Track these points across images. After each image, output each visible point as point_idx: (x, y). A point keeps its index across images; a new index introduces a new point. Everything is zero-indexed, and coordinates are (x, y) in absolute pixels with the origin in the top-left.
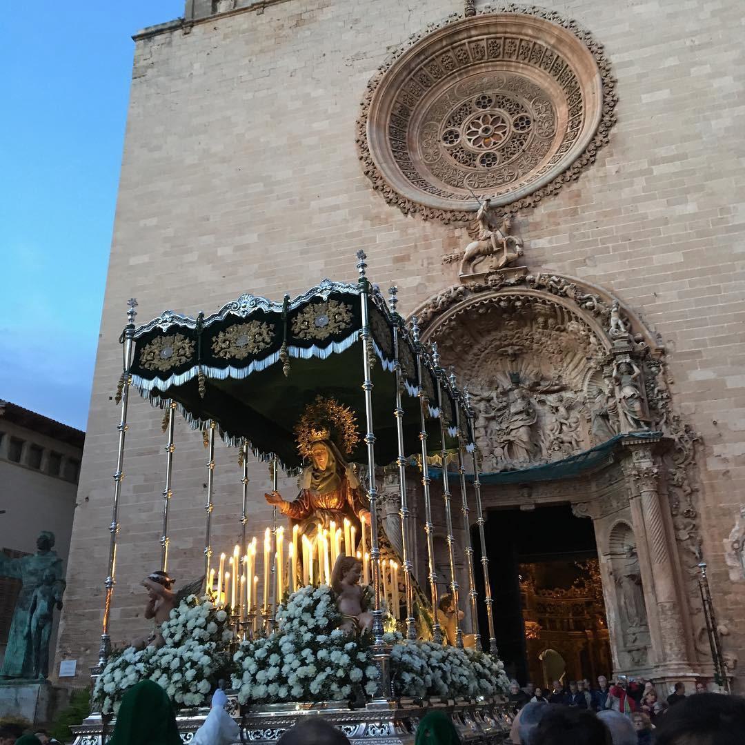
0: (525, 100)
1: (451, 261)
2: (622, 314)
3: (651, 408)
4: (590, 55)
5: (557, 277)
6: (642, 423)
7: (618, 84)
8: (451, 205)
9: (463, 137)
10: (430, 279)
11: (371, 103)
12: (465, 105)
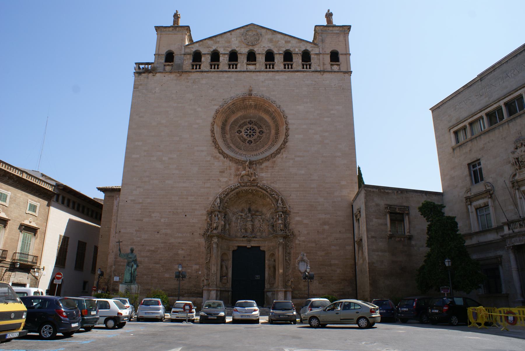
0: (263, 125)
1: (237, 175)
2: (282, 200)
3: (285, 226)
4: (284, 119)
5: (266, 186)
6: (282, 230)
7: (290, 130)
8: (238, 158)
9: (243, 133)
10: (230, 180)
11: (217, 118)
12: (244, 122)
